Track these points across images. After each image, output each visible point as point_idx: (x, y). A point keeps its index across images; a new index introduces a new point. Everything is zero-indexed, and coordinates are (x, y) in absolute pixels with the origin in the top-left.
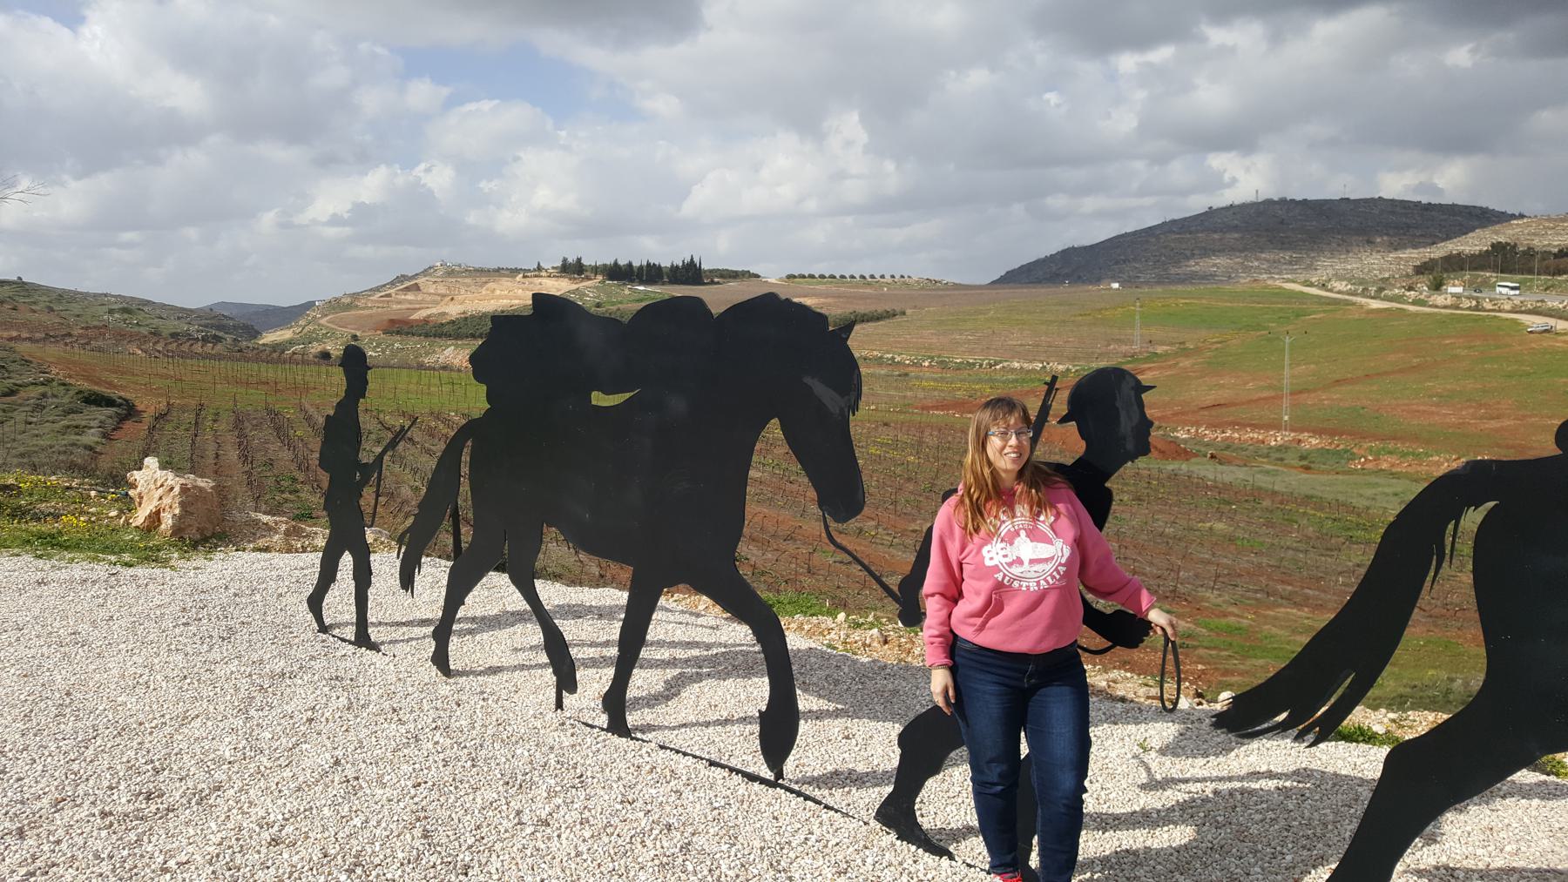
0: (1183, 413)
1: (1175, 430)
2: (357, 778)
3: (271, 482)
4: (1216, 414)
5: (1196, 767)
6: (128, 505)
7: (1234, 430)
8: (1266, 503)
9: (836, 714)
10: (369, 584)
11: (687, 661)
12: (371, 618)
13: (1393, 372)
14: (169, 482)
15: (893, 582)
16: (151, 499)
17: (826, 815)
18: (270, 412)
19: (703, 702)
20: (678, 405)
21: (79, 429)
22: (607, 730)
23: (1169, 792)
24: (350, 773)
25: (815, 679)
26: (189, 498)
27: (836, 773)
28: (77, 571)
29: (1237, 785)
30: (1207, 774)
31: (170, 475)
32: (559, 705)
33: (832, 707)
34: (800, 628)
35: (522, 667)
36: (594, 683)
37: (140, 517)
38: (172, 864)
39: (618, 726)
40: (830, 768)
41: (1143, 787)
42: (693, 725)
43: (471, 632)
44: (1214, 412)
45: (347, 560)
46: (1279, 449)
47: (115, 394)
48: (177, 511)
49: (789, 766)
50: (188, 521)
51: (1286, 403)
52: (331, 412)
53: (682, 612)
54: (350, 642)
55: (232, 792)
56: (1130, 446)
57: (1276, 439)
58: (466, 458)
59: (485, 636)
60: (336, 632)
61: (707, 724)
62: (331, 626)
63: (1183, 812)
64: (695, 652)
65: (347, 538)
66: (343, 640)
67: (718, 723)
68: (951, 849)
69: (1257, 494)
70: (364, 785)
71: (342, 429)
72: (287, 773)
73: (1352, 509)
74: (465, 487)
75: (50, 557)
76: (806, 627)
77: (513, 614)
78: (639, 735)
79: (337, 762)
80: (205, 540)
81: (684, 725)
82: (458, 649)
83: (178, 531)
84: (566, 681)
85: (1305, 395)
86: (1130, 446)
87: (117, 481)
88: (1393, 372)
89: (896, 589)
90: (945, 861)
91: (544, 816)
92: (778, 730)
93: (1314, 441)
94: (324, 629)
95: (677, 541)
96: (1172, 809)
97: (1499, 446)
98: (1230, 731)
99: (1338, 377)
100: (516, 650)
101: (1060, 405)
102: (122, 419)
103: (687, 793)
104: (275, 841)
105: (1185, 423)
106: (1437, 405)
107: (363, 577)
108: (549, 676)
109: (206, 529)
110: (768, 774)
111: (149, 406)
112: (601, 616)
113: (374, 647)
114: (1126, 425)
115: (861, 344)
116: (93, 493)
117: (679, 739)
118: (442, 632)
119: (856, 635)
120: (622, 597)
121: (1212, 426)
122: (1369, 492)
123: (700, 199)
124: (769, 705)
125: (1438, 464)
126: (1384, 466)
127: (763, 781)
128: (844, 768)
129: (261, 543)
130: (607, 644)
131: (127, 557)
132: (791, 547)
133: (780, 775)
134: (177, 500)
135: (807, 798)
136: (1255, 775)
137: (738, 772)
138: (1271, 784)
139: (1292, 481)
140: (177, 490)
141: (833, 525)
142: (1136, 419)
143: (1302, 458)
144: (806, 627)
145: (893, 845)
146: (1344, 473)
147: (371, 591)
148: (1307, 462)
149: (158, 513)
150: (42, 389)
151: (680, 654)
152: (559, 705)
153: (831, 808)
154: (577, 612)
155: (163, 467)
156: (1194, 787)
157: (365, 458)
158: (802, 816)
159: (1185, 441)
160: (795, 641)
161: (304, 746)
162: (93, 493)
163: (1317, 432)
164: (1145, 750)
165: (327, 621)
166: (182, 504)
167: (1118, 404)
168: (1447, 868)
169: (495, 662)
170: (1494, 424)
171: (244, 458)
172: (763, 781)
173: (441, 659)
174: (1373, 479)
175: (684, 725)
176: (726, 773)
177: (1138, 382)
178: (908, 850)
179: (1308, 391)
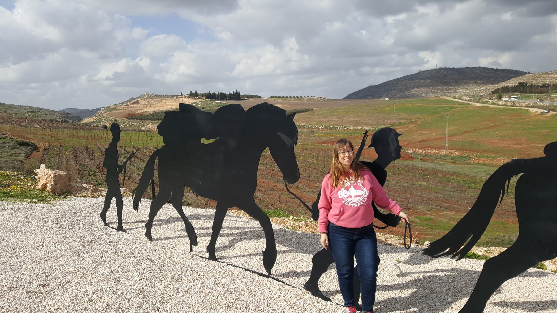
0: (410, 144)
1: (408, 150)
2: (119, 278)
3: (86, 172)
4: (422, 144)
5: (417, 268)
6: (35, 181)
7: (428, 150)
8: (440, 175)
9: (290, 251)
10: (122, 208)
11: (237, 234)
12: (123, 221)
13: (484, 128)
14: (50, 173)
15: (310, 205)
16: (43, 179)
17: (287, 287)
18: (86, 147)
19: (243, 248)
20: (232, 143)
21: (17, 155)
22: (209, 259)
23: (407, 277)
24: (117, 276)
25: (282, 239)
27: (290, 272)
28: (17, 205)
29: (431, 274)
30: (420, 270)
31: (50, 170)
32: (191, 250)
33: (288, 249)
34: (277, 221)
35: (178, 237)
36: (204, 242)
37: (39, 185)
38: (52, 309)
39: (212, 257)
40: (288, 271)
41: (398, 275)
42: (239, 256)
43: (159, 225)
45: (114, 200)
46: (444, 156)
47: (30, 142)
48: (53, 183)
49: (273, 270)
50: (56, 187)
51: (447, 140)
52: (107, 147)
53: (235, 217)
54: (116, 229)
55: (74, 283)
56: (393, 155)
57: (443, 152)
58: (156, 163)
59: (164, 226)
60: (111, 225)
61: (244, 256)
62: (109, 224)
63: (413, 283)
64: (240, 231)
65: (114, 192)
66: (113, 228)
67: (248, 255)
68: (331, 298)
69: (436, 172)
70: (121, 280)
71: (111, 153)
72: (94, 276)
73: (470, 177)
74: (156, 173)
75: (7, 200)
76: (279, 221)
77: (174, 218)
78: (220, 260)
79: (112, 272)
80: (63, 193)
81: (236, 256)
82: (155, 231)
83: (53, 190)
84: (194, 242)
85: (453, 137)
86: (393, 155)
87: (31, 173)
88: (484, 128)
89: (311, 207)
90: (329, 303)
91: (186, 290)
92: (269, 258)
93: (456, 153)
94: (106, 224)
95: (233, 192)
96: (408, 283)
97: (521, 154)
98: (429, 255)
99: (465, 130)
100: (176, 231)
101: (369, 141)
102: (33, 151)
103: (237, 280)
104: (90, 301)
105: (411, 147)
106: (500, 140)
107: (120, 206)
108: (187, 240)
109: (63, 189)
110: (266, 273)
111: (42, 146)
112: (206, 219)
113: (124, 231)
114: (392, 148)
115: (298, 120)
116: (22, 177)
117: (234, 261)
118: (149, 225)
119: (297, 224)
120: (213, 212)
121: (421, 148)
122: (475, 171)
123: (239, 69)
124: (266, 249)
125: (500, 161)
126: (481, 161)
127: (264, 276)
128: (293, 270)
129: (83, 194)
130: (208, 228)
131: (35, 200)
132: (273, 193)
133: (270, 273)
134: (53, 179)
135: (280, 281)
136: (437, 271)
137: (255, 272)
138: (443, 274)
139: (449, 167)
140: (52, 176)
141: (288, 185)
142: (396, 146)
143: (452, 159)
144: (279, 221)
145: (310, 297)
146: (467, 164)
147: (123, 211)
148: (454, 161)
149: (46, 184)
150: (3, 140)
151: (234, 231)
152: (191, 250)
153: (288, 285)
154: (197, 217)
155: (47, 168)
156: (416, 275)
157: (120, 163)
158: (278, 287)
159: (411, 154)
160: (275, 226)
161: (100, 267)
162: (22, 177)
163: (457, 150)
164: (399, 262)
165: (107, 222)
166: (54, 181)
167: (389, 140)
168: (504, 302)
169: (168, 235)
170: (519, 146)
171: (77, 164)
172: (264, 276)
173: (148, 235)
174: (477, 166)
175: (236, 256)
176: (251, 273)
177: (396, 133)
178: (315, 299)
179: (454, 135)
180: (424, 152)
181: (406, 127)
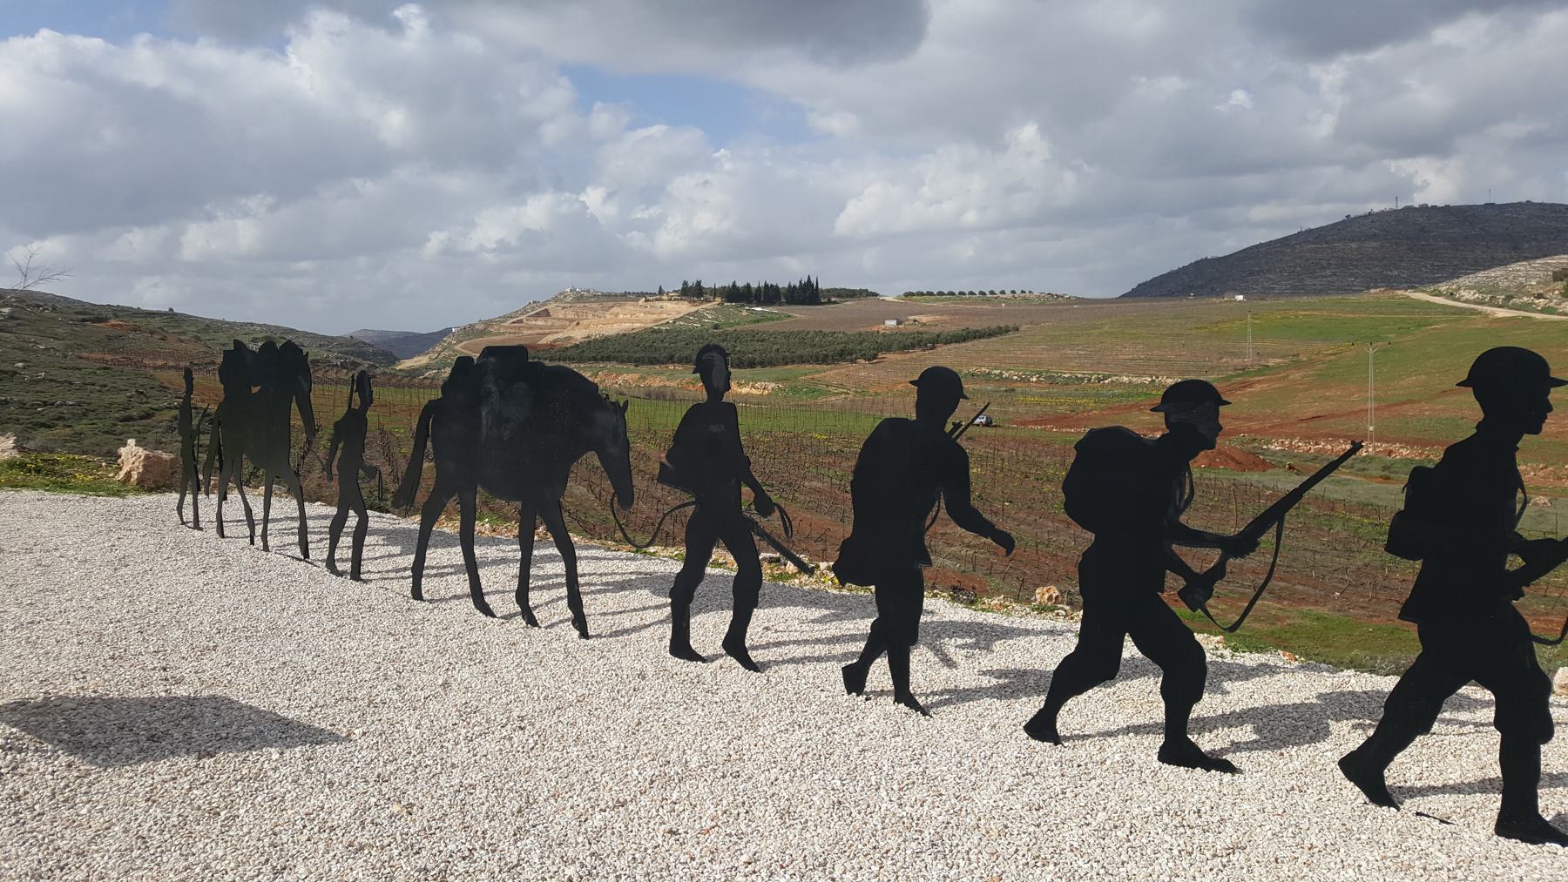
7: (1327, 442)
26: (149, 463)
36: (259, 530)
37: (122, 474)
44: (1312, 424)
83: (140, 481)
121: (1306, 438)
159: (1275, 453)
179: (1411, 402)
180: (1313, 448)
181: (1279, 380)
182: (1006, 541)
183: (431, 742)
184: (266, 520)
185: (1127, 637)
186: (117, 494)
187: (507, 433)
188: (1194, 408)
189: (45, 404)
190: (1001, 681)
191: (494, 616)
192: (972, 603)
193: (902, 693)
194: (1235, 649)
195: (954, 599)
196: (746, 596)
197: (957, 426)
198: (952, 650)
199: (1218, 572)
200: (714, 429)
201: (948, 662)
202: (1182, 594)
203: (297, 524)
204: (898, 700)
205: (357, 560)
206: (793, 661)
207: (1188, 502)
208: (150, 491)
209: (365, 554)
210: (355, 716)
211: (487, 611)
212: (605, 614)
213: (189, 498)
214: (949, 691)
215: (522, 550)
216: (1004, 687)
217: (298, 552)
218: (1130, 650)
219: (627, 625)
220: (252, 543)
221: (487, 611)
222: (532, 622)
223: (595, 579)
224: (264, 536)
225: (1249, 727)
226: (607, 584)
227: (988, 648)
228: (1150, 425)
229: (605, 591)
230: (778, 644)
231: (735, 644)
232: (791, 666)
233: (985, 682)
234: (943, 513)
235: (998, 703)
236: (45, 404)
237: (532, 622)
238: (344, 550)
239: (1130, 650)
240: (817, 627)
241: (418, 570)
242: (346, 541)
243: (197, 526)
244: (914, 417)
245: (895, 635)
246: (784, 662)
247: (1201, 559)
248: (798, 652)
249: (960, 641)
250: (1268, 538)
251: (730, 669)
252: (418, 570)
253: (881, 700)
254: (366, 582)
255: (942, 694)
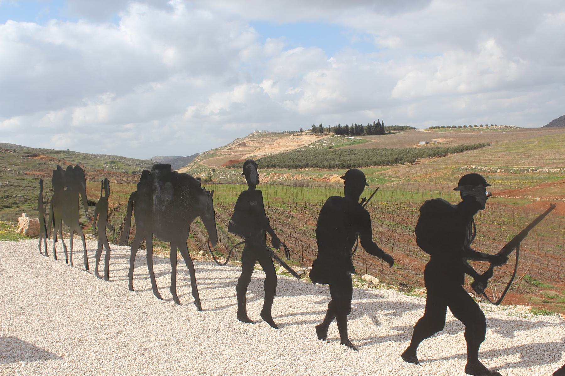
31: (28, 218)
37: (19, 230)
83: (27, 234)
110: (85, 269)
113: (48, 256)
166: (29, 226)
182: (390, 260)
183: (98, 360)
184: (72, 251)
185: (448, 309)
186: (15, 239)
187: (163, 208)
188: (473, 186)
189: (8, 197)
190: (400, 332)
191: (162, 299)
192: (409, 291)
193: (345, 340)
194: (536, 313)
195: (400, 290)
196: (270, 289)
197: (364, 200)
198: (381, 316)
199: (489, 274)
200: (252, 204)
201: (377, 323)
202: (473, 285)
203: (83, 254)
204: (342, 343)
205: (107, 271)
206: (297, 323)
207: (473, 238)
208: (32, 238)
209: (111, 268)
210: (70, 347)
211: (160, 297)
212: (215, 299)
213: (43, 240)
214: (372, 338)
215: (187, 265)
216: (400, 335)
217: (84, 267)
218: (449, 316)
219: (224, 304)
220: (67, 262)
221: (160, 297)
222: (178, 302)
223: (217, 281)
224: (71, 259)
225: (518, 355)
226: (222, 283)
227: (400, 316)
228: (454, 198)
229: (219, 287)
230: (293, 314)
231: (266, 315)
232: (295, 326)
233: (392, 333)
234: (360, 245)
235: (394, 343)
236: (8, 197)
237: (178, 302)
238: (102, 267)
239: (449, 316)
240: (316, 305)
241: (131, 276)
242: (102, 262)
243: (47, 254)
244: (343, 196)
245: (339, 310)
246: (291, 324)
247: (480, 267)
248: (301, 318)
249: (386, 312)
250: (512, 256)
251: (265, 326)
252: (131, 276)
253: (335, 343)
254: (110, 281)
255: (368, 339)
